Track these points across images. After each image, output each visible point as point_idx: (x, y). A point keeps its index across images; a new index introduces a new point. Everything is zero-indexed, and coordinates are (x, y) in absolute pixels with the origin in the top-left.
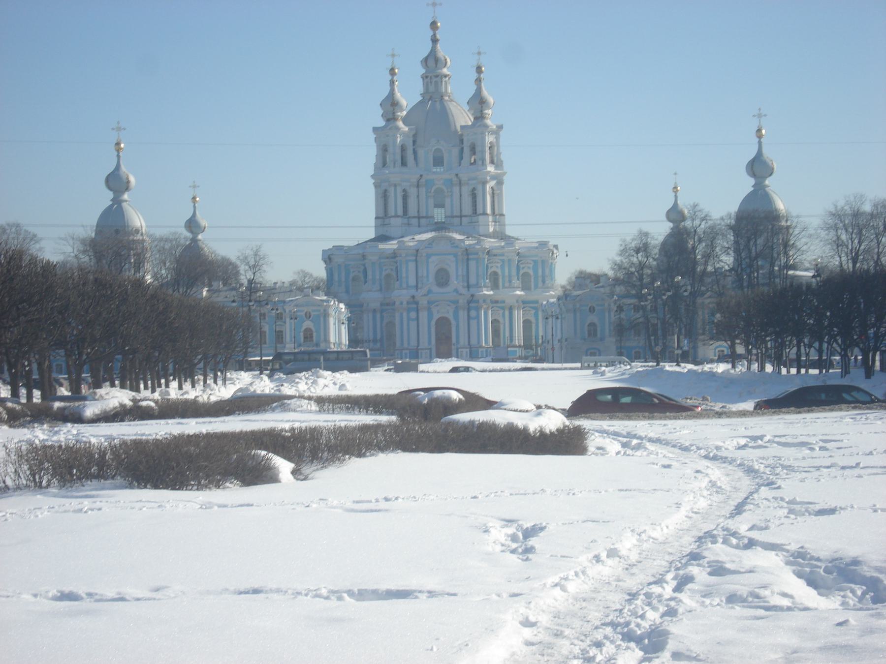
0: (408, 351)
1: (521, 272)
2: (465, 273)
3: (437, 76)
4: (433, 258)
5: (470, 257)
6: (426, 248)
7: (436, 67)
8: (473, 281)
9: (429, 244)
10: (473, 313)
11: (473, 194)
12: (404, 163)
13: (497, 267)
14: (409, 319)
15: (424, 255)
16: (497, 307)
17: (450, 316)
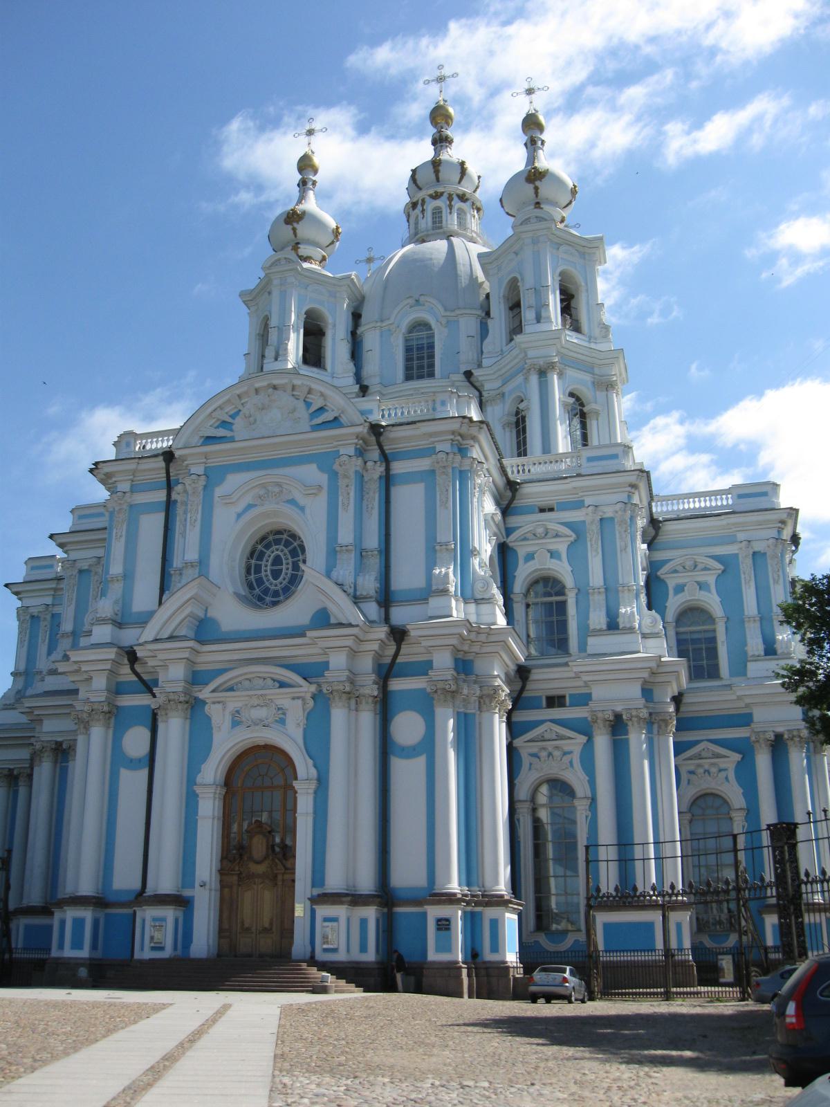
0: (87, 914)
1: (674, 604)
2: (372, 541)
3: (436, 196)
4: (233, 481)
5: (398, 467)
6: (209, 440)
7: (438, 180)
8: (406, 577)
9: (224, 424)
10: (407, 727)
11: (517, 424)
12: (313, 355)
13: (554, 554)
14: (118, 760)
15: (199, 470)
16: (553, 721)
17: (290, 740)
